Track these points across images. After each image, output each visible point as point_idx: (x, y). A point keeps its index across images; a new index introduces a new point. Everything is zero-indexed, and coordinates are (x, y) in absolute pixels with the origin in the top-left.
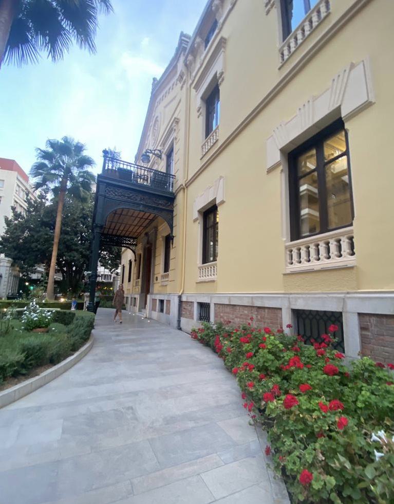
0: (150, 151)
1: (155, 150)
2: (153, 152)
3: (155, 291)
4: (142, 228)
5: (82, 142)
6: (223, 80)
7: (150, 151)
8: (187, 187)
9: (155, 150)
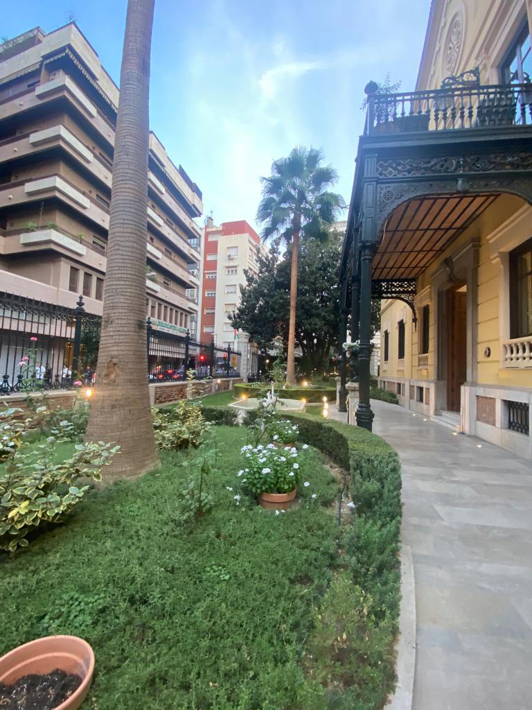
1: (462, 75)
3: (481, 380)
4: (431, 254)
7: (451, 81)
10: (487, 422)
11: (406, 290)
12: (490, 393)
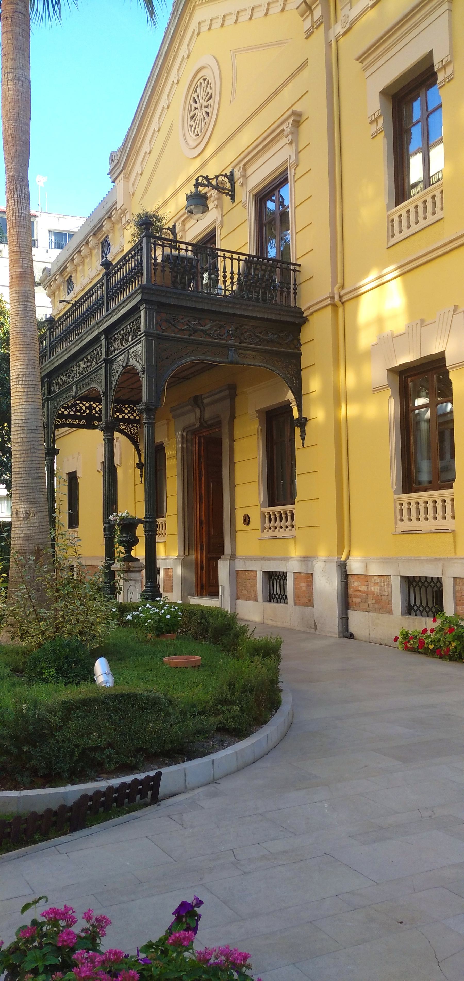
0: (206, 182)
2: (214, 182)
3: (241, 551)
7: (206, 182)
8: (343, 303)
9: (217, 177)
10: (248, 599)
11: (126, 417)
12: (251, 566)
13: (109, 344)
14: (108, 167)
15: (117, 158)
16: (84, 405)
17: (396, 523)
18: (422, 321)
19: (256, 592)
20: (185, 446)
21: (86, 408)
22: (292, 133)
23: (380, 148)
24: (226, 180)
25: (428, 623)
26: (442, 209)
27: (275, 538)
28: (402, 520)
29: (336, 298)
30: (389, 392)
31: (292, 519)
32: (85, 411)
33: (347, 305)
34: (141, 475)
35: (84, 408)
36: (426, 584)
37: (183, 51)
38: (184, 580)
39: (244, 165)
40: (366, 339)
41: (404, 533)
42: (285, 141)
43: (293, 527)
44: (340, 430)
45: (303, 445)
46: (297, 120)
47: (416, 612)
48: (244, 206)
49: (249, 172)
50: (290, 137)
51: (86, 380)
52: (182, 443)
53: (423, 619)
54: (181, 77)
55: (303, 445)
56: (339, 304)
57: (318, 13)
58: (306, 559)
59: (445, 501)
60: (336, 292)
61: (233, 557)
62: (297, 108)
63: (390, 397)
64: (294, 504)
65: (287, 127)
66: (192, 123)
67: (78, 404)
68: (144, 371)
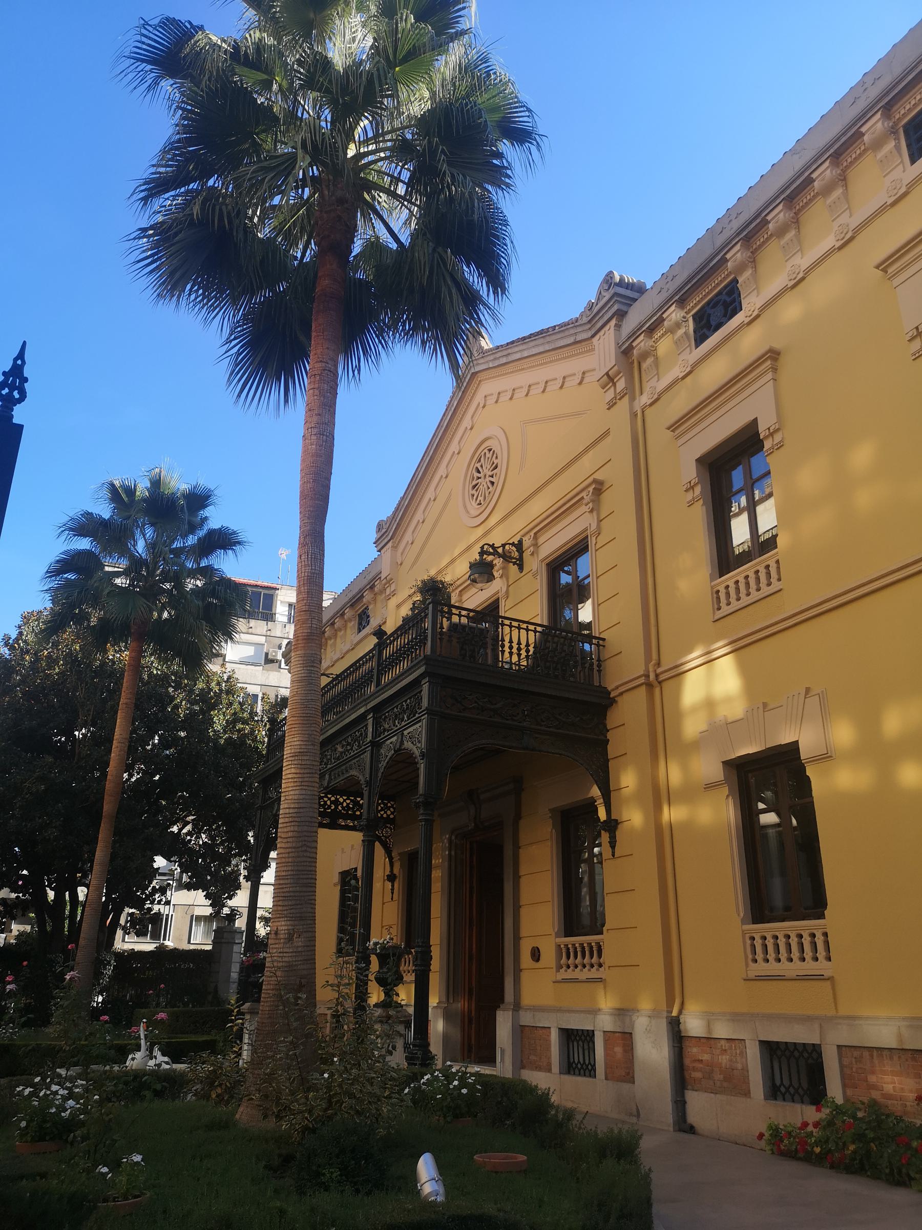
2: (500, 550)
3: (527, 999)
5: (204, 481)
6: (780, 446)
8: (660, 683)
9: (503, 546)
12: (543, 1021)
13: (377, 723)
14: (374, 536)
15: (385, 527)
16: (329, 799)
17: (747, 965)
18: (765, 705)
19: (550, 1058)
20: (453, 853)
21: (332, 802)
22: (593, 501)
23: (698, 517)
24: (514, 548)
25: (811, 1114)
26: (779, 580)
27: (576, 981)
28: (791, 960)
29: (652, 676)
30: (725, 790)
31: (600, 956)
32: (330, 807)
33: (665, 685)
34: (393, 889)
35: (328, 803)
36: (796, 1054)
37: (467, 423)
38: (446, 1038)
39: (535, 534)
40: (693, 727)
41: (759, 978)
42: (583, 509)
43: (600, 965)
44: (663, 838)
45: (613, 855)
46: (599, 488)
47: (784, 1095)
48: (535, 576)
49: (541, 540)
50: (591, 505)
51: (344, 767)
52: (450, 851)
53: (798, 1106)
54: (462, 449)
55: (613, 855)
56: (656, 683)
57: (621, 384)
58: (622, 1013)
59: (789, 937)
60: (651, 669)
61: (517, 1007)
62: (598, 476)
63: (728, 796)
64: (602, 933)
65: (587, 496)
66: (474, 492)
67: (322, 798)
68: (423, 756)
